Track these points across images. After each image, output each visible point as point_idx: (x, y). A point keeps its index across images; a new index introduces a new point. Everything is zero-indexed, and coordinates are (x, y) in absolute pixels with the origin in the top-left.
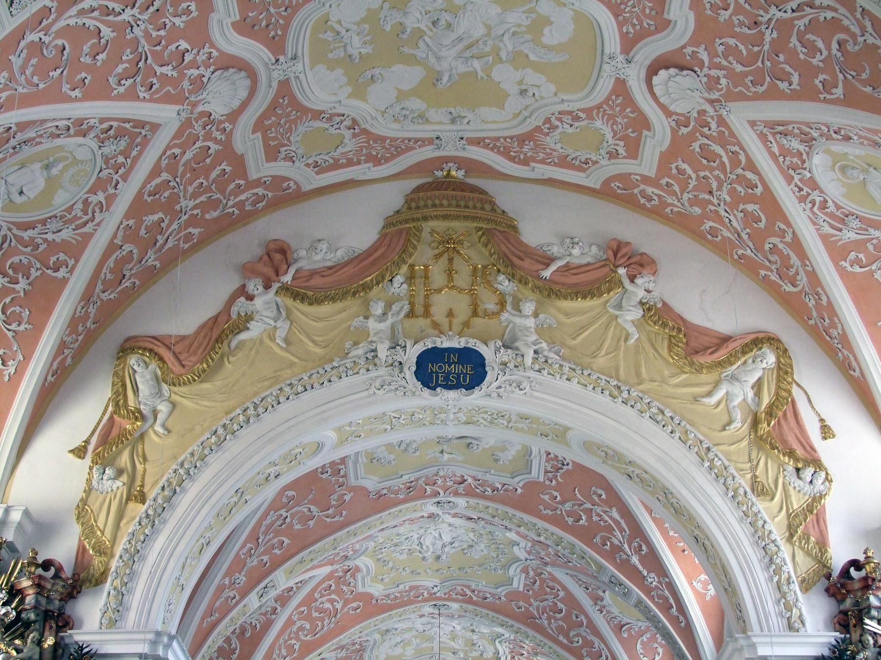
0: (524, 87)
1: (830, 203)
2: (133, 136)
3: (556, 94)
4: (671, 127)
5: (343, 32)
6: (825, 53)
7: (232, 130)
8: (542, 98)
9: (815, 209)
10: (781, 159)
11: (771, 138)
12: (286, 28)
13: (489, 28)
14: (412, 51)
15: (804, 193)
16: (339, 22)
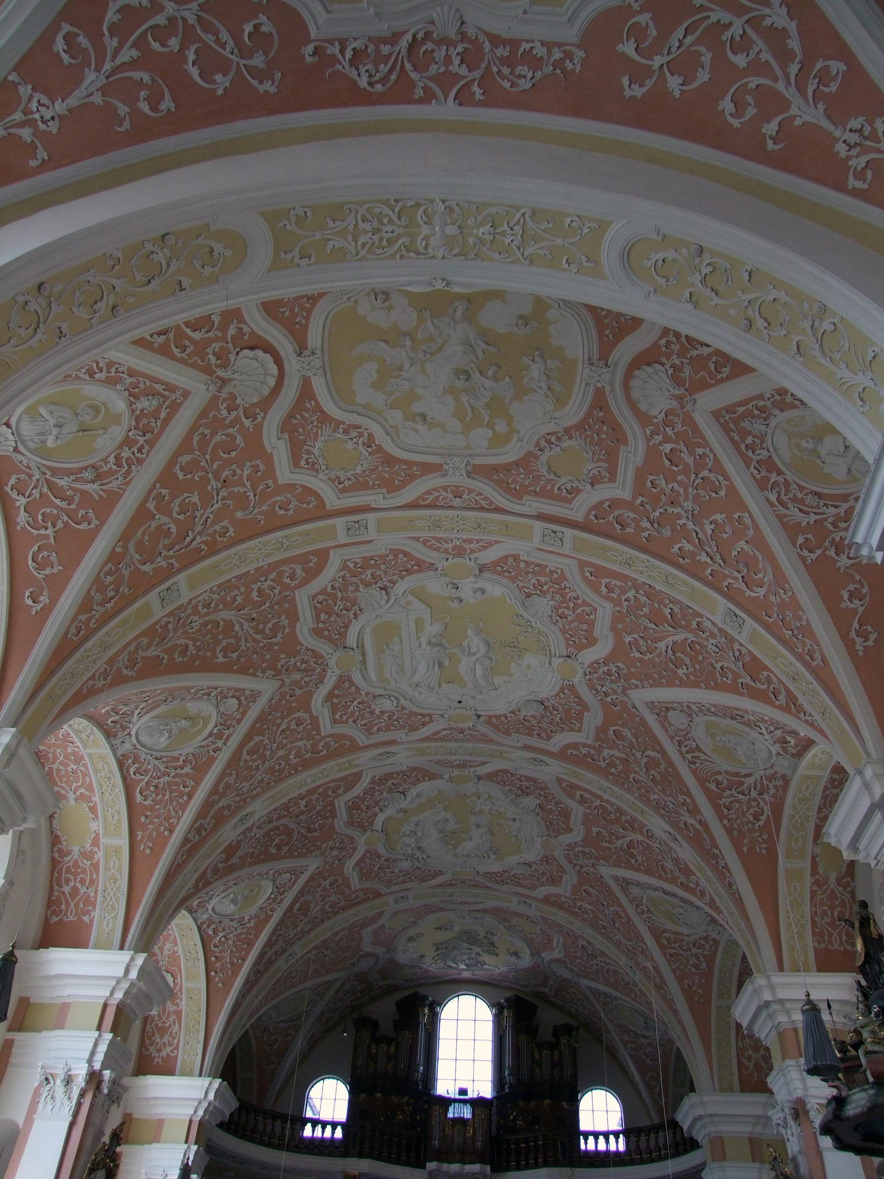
0: (386, 304)
1: (87, 377)
2: (736, 421)
3: (356, 302)
4: (245, 322)
5: (545, 388)
6: (175, 515)
7: (660, 338)
8: (367, 295)
9: (95, 365)
10: (148, 383)
11: (166, 393)
12: (589, 414)
13: (424, 371)
14: (490, 348)
15: (113, 370)
16: (547, 396)
